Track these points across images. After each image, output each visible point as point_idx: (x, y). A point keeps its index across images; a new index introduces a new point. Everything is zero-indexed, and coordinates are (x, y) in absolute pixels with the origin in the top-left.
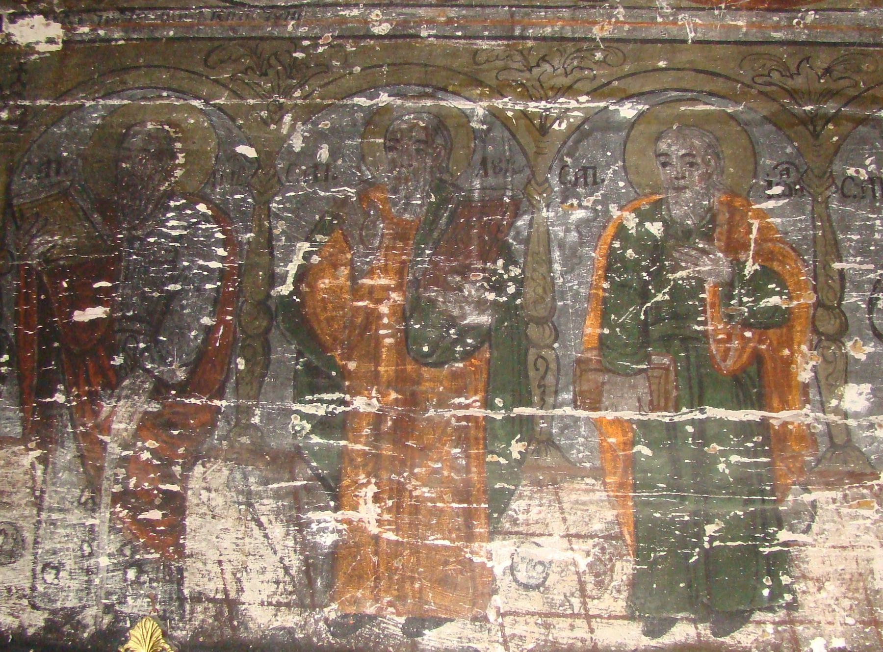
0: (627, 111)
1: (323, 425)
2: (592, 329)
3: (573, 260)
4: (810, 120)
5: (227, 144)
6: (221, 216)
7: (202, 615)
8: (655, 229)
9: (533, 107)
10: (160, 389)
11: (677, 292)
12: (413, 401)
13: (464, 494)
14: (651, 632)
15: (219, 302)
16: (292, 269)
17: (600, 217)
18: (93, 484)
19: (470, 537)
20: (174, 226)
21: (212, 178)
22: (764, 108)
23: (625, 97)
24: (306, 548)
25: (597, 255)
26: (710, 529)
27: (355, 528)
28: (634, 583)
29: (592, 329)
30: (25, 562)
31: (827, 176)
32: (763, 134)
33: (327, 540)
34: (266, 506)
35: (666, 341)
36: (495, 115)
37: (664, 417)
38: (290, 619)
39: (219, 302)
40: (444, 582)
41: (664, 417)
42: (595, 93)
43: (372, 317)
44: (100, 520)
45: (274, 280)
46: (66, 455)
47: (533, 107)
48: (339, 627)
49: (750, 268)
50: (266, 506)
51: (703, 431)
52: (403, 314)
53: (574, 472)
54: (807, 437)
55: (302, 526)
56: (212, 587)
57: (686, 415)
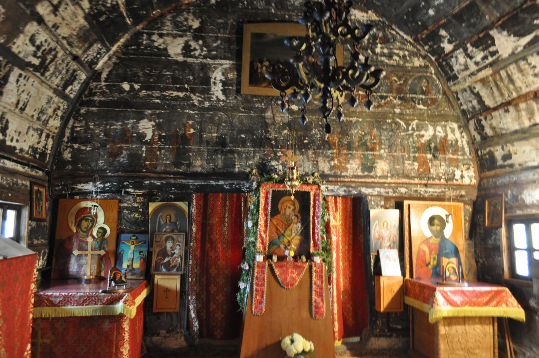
0: (360, 120)
1: (331, 153)
2: (357, 144)
3: (355, 136)
4: (380, 122)
5: (318, 123)
6: (319, 131)
7: (321, 172)
8: (363, 133)
9: (351, 119)
10: (314, 149)
11: (365, 140)
12: (340, 151)
13: (345, 160)
14: (363, 173)
15: (319, 140)
16: (327, 137)
17: (358, 132)
18: (308, 159)
19: (346, 164)
20: (314, 132)
21: (317, 126)
22: (374, 120)
23: (360, 118)
24: (331, 165)
25: (357, 136)
26: (368, 164)
27: (335, 164)
28: (362, 169)
29: (357, 144)
30: (302, 168)
31: (381, 128)
32: (374, 123)
33: (332, 165)
34: (326, 162)
35: (364, 145)
36: (347, 120)
37: (364, 153)
38: (329, 172)
39: (319, 140)
40: (344, 169)
41: (364, 153)
42: (357, 117)
43: (335, 142)
44: (310, 163)
45: (325, 138)
46: (305, 156)
47: (351, 119)
48: (334, 173)
49: (373, 138)
50: (326, 162)
51: (368, 154)
52: (338, 142)
53: (355, 158)
54: (378, 155)
55: (330, 164)
56: (322, 169)
57: (366, 153)
